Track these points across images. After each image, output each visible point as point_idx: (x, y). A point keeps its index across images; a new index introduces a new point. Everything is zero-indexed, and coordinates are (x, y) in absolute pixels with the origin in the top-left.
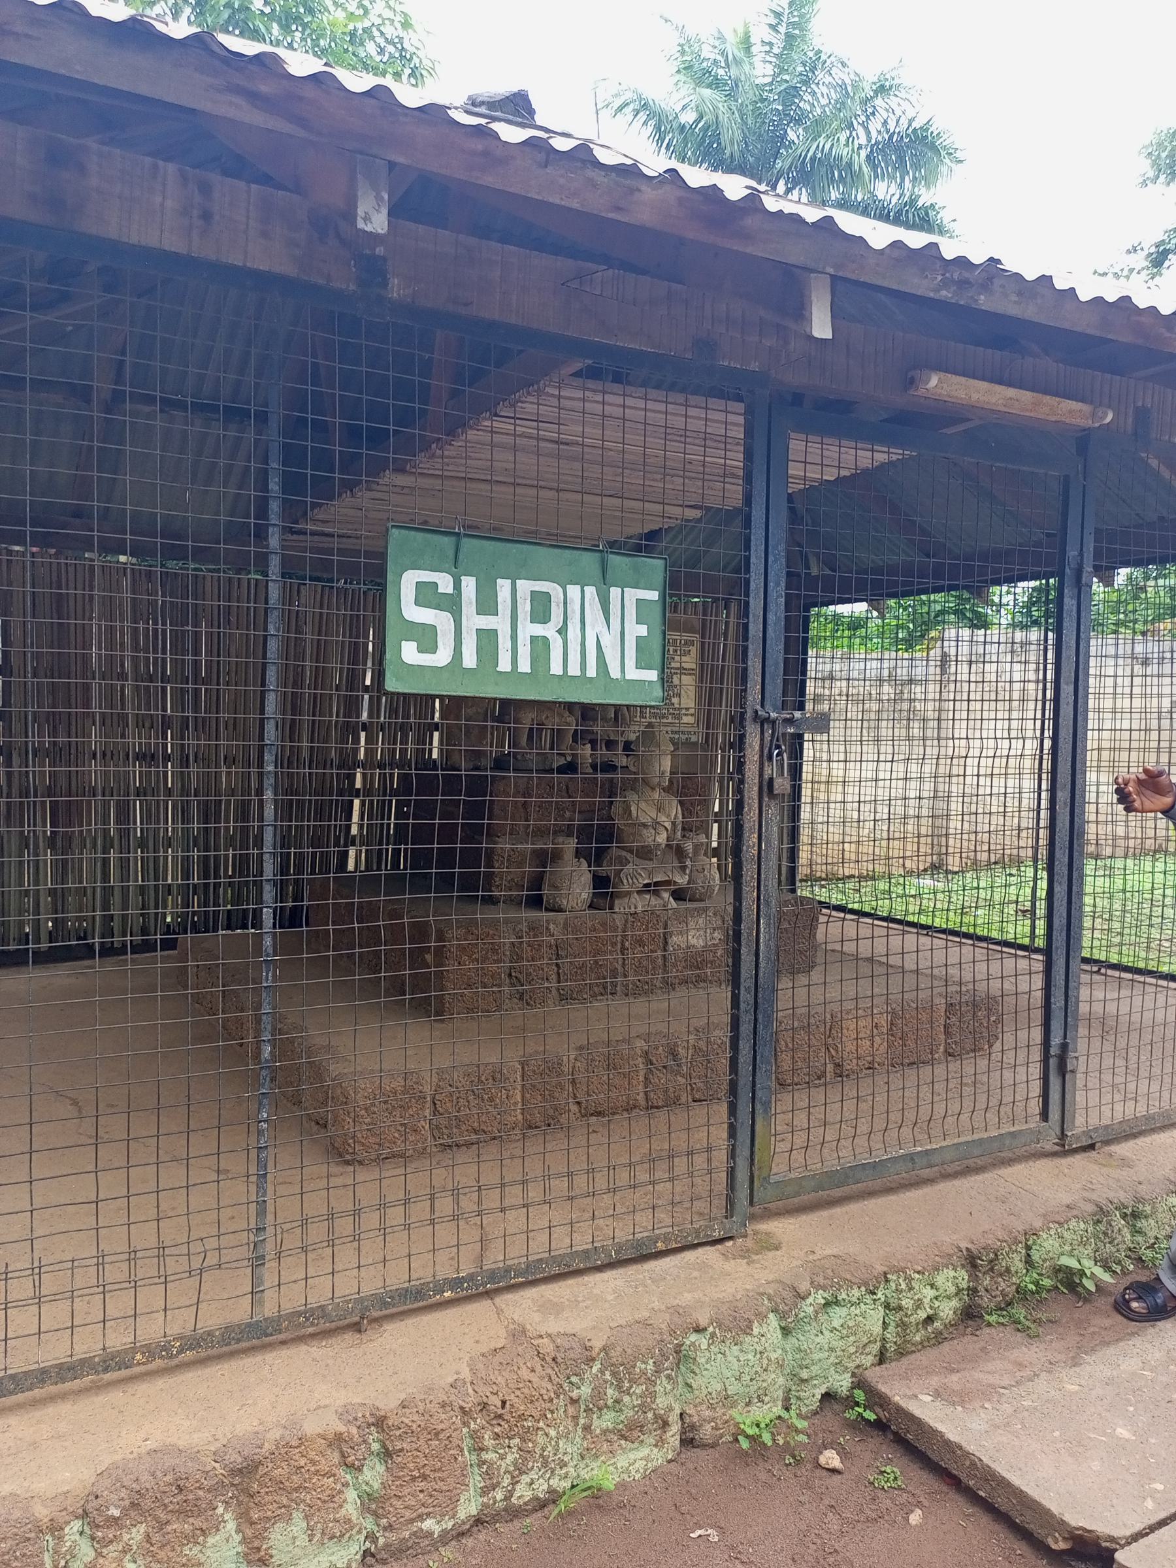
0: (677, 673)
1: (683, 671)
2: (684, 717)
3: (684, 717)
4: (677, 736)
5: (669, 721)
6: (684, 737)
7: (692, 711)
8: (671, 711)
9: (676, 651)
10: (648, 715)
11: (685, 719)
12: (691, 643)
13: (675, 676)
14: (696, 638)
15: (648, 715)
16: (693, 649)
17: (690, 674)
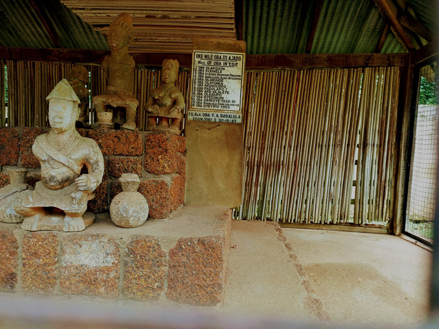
0: (226, 78)
1: (232, 77)
2: (231, 107)
3: (231, 107)
4: (225, 119)
5: (219, 109)
6: (230, 120)
7: (238, 102)
8: (221, 102)
9: (226, 64)
10: (203, 105)
11: (232, 108)
12: (239, 59)
13: (224, 80)
14: (242, 56)
15: (203, 105)
16: (240, 63)
17: (237, 79)
